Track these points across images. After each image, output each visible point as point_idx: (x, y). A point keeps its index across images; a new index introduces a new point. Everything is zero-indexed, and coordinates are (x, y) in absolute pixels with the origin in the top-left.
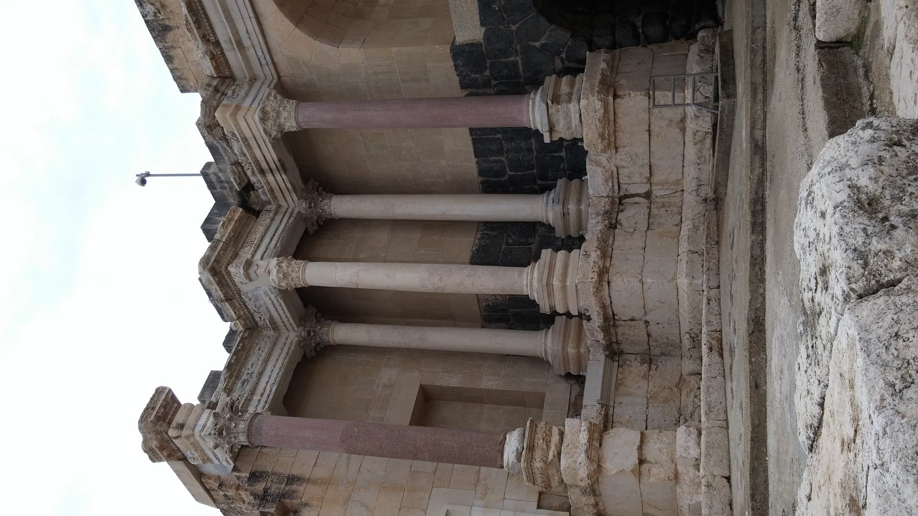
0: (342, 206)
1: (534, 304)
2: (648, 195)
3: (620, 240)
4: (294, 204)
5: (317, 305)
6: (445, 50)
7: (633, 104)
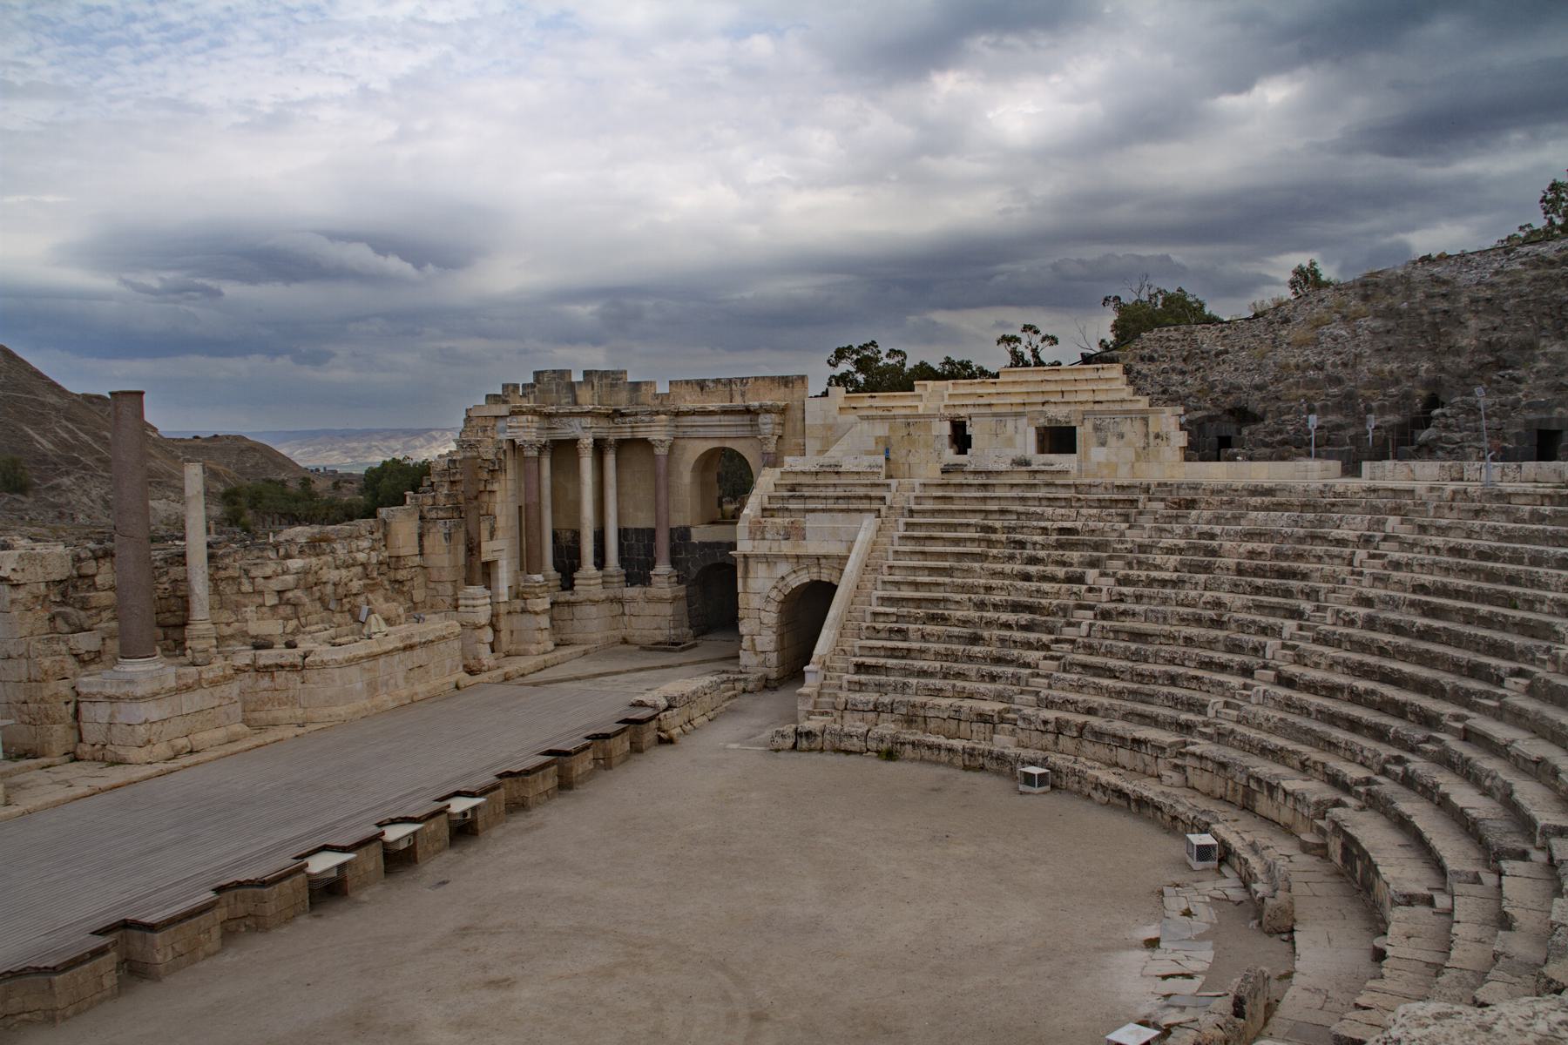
0: (610, 460)
2: (623, 614)
3: (606, 606)
4: (612, 438)
5: (563, 450)
7: (667, 609)
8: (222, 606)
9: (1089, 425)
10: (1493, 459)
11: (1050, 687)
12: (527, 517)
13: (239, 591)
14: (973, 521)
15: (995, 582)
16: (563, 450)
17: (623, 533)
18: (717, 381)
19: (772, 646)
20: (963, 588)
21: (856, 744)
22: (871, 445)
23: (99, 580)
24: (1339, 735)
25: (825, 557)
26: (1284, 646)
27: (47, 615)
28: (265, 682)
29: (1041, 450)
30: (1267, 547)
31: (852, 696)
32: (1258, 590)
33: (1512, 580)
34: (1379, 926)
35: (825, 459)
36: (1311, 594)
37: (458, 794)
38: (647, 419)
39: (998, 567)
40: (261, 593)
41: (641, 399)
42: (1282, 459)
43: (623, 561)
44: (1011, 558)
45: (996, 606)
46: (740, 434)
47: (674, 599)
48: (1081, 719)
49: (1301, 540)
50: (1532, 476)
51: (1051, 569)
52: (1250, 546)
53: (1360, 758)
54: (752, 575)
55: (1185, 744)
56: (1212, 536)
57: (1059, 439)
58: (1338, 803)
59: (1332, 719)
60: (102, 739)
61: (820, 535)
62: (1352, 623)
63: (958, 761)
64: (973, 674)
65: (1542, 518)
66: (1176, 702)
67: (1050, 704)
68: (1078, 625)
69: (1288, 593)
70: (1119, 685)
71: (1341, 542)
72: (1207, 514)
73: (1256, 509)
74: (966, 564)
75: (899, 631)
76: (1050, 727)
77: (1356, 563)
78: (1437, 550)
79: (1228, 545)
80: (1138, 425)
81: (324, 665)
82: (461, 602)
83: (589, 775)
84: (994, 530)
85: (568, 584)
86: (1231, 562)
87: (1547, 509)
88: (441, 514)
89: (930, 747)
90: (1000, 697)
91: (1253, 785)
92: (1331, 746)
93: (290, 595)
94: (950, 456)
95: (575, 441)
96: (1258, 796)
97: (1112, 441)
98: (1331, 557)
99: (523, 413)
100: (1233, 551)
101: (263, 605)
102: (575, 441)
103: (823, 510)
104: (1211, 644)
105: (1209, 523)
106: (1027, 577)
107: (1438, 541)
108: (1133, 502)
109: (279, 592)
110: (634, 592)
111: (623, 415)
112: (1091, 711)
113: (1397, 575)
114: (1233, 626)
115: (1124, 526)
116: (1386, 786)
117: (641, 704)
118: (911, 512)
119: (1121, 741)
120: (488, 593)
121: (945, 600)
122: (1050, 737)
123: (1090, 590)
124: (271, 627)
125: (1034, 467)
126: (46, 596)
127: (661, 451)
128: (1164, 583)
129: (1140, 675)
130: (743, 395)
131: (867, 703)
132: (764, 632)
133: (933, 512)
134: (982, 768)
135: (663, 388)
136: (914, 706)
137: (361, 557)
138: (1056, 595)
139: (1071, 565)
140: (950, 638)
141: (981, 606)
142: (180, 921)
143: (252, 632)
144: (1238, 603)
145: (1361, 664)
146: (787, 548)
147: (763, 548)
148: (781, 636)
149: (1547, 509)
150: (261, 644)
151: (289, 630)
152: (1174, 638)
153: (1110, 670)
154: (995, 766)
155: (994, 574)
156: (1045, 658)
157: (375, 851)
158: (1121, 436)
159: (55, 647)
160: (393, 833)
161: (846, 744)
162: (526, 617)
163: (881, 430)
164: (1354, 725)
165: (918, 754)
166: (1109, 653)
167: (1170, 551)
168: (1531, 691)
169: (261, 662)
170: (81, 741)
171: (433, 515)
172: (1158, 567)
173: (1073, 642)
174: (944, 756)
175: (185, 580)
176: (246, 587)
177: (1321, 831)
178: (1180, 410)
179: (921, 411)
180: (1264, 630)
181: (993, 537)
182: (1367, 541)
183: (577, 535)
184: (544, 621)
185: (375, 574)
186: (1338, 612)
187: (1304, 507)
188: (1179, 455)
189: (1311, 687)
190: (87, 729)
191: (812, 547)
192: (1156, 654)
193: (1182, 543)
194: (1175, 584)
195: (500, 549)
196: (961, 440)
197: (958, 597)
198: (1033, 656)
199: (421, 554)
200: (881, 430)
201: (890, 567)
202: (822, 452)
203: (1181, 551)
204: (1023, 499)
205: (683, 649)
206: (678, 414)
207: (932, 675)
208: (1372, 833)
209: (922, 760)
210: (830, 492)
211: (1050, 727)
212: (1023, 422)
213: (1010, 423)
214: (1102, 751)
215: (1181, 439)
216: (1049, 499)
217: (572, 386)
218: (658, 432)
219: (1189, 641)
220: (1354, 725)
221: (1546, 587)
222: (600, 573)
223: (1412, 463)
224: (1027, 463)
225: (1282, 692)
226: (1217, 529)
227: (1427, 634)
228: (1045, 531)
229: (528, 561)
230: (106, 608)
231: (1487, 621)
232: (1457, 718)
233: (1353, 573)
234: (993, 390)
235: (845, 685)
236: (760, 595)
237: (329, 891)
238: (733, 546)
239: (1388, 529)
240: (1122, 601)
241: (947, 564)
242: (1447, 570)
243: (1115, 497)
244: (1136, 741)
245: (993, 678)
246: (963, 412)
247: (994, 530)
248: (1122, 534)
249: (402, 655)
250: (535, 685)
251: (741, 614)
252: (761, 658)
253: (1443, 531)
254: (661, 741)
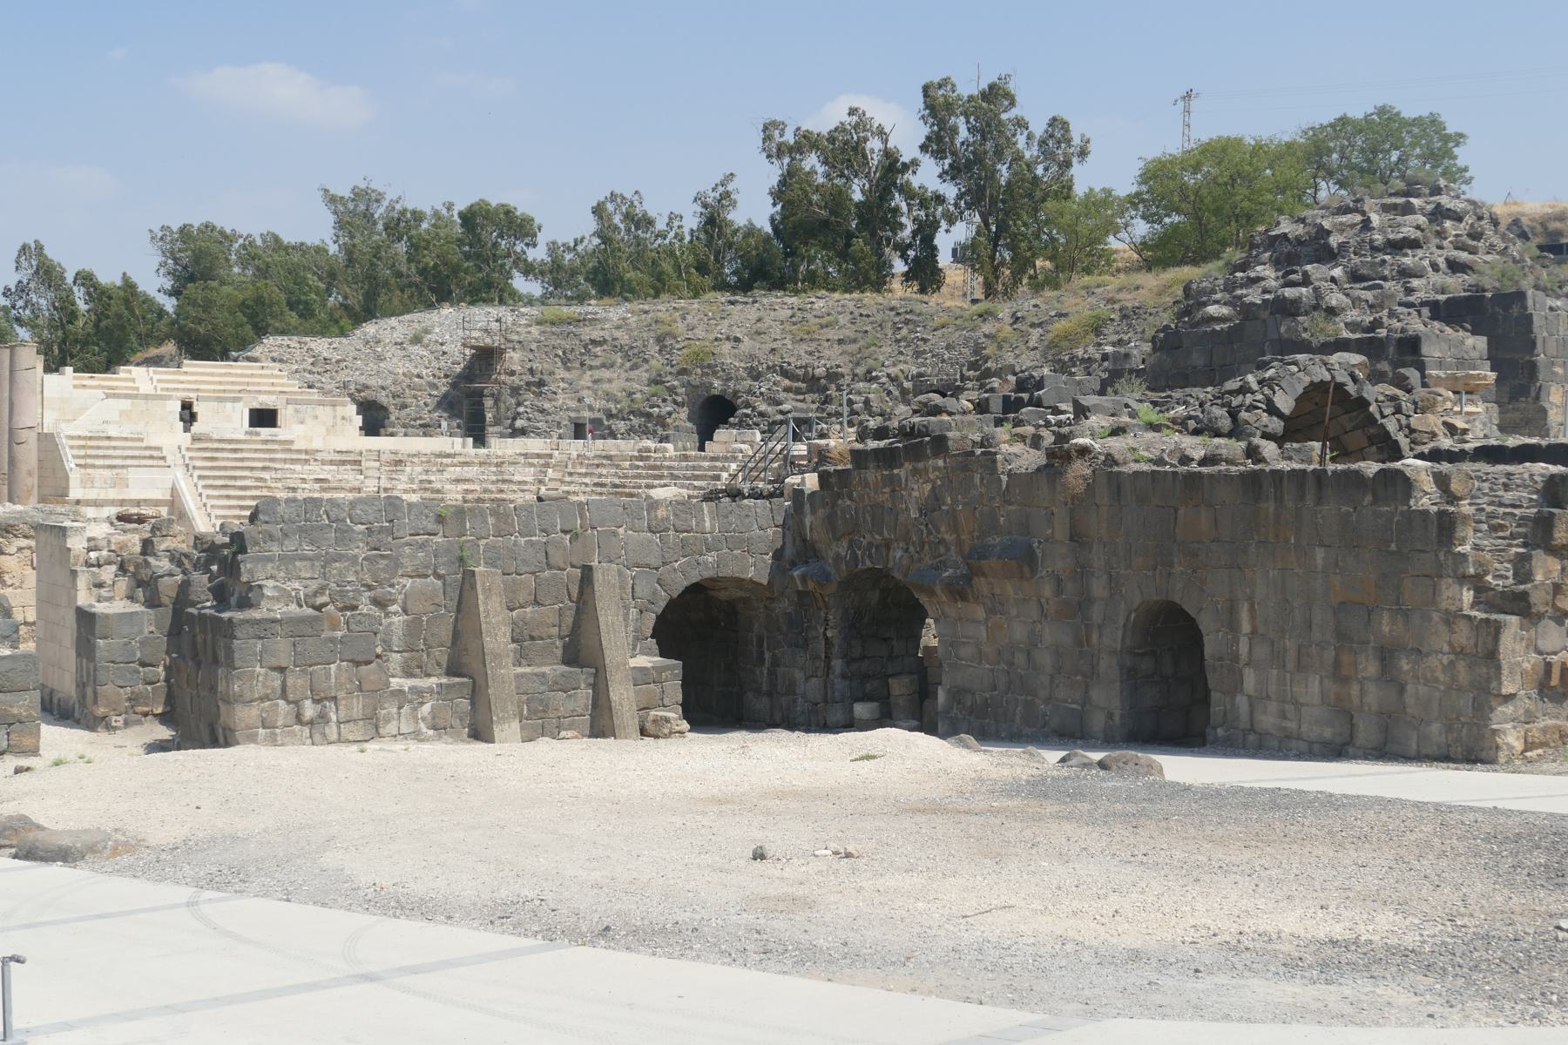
42: (425, 435)
57: (263, 418)
65: (638, 467)
71: (525, 483)
97: (309, 421)
107: (587, 480)
108: (358, 463)
125: (263, 437)
147: (92, 494)
167: (405, 491)
182: (541, 482)
187: (481, 464)
191: (134, 493)
196: (188, 414)
200: (125, 404)
212: (239, 405)
213: (229, 405)
215: (359, 420)
226: (433, 478)
246: (193, 395)
253: (586, 475)
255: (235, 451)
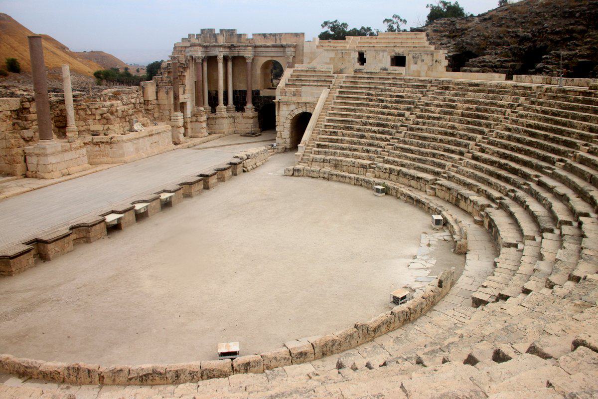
0: (230, 64)
1: (217, 106)
2: (234, 122)
4: (230, 56)
6: (259, 89)
7: (251, 121)
8: (80, 120)
9: (411, 56)
10: (563, 76)
11: (388, 155)
12: (198, 86)
13: (86, 114)
14: (364, 91)
15: (371, 115)
16: (211, 61)
17: (233, 91)
18: (271, 34)
19: (288, 136)
20: (359, 117)
21: (315, 175)
22: (328, 61)
23: (31, 110)
24: (493, 180)
25: (308, 103)
26: (476, 145)
27: (12, 123)
28: (97, 148)
29: (392, 65)
30: (473, 106)
31: (315, 156)
32: (469, 123)
33: (564, 124)
34: (497, 253)
35: (310, 66)
36: (488, 126)
37: (165, 191)
38: (243, 48)
39: (372, 109)
40: (94, 115)
41: (242, 41)
42: (483, 72)
43: (235, 102)
44: (378, 106)
45: (371, 124)
46: (279, 55)
47: (253, 117)
48: (398, 168)
49: (487, 104)
50: (577, 84)
51: (392, 111)
52: (467, 105)
53: (499, 189)
54: (281, 109)
55: (436, 180)
56: (454, 101)
57: (399, 61)
58: (489, 206)
59: (491, 174)
60: (34, 169)
61: (307, 94)
62: (502, 138)
63: (353, 182)
64: (360, 149)
66: (434, 164)
67: (388, 162)
68: (401, 132)
69: (480, 125)
70: (414, 156)
72: (453, 92)
73: (471, 91)
74: (360, 108)
75: (334, 132)
76: (387, 171)
77: (506, 114)
78: (537, 111)
79: (459, 105)
80: (430, 57)
81: (118, 142)
82: (172, 118)
83: (215, 185)
84: (372, 95)
85: (214, 111)
86: (459, 111)
87: (580, 97)
88: (164, 84)
89: (342, 177)
90: (369, 158)
91: (459, 197)
92: (489, 184)
93: (105, 115)
94: (357, 66)
95: (216, 57)
96: (461, 201)
98: (498, 111)
99: (195, 46)
100: (461, 107)
101: (95, 119)
102: (216, 57)
103: (309, 85)
104: (449, 143)
105: (453, 96)
106: (383, 114)
107: (538, 107)
108: (425, 87)
109: (101, 115)
110: (239, 114)
111: (235, 47)
112: (403, 165)
113: (521, 120)
114: (458, 136)
115: (421, 95)
116: (507, 201)
117: (237, 157)
118: (342, 87)
119: (413, 177)
120: (182, 114)
121: (352, 121)
122: (387, 175)
123: (406, 119)
124: (98, 127)
125: (389, 71)
126: (11, 116)
127: (249, 61)
128: (434, 118)
129: (422, 153)
130: (280, 40)
131: (321, 159)
132: (285, 131)
133: (349, 87)
134: (361, 185)
135: (250, 37)
136: (338, 161)
137: (133, 101)
138: (394, 121)
139: (400, 110)
140: (353, 136)
141: (365, 124)
142: (61, 238)
143: (91, 129)
144: (461, 127)
145: (504, 153)
146: (294, 99)
147: (284, 99)
148: (292, 132)
149: (580, 97)
150: (95, 133)
151: (105, 128)
152: (436, 140)
153: (411, 150)
154: (365, 185)
155: (371, 112)
156: (388, 145)
157: (132, 213)
158: (423, 61)
159: (15, 135)
160: (138, 207)
161: (312, 174)
162: (197, 123)
163: (332, 55)
164: (499, 177)
165: (337, 179)
166: (412, 144)
167: (437, 106)
168: (565, 168)
169: (95, 141)
170: (28, 170)
171: (161, 84)
172: (432, 112)
173: (398, 139)
174: (347, 180)
175: (65, 110)
176: (89, 112)
177: (482, 216)
178: (446, 51)
179: (348, 48)
180: (469, 139)
181: (371, 97)
182: (511, 106)
183: (217, 93)
184: (204, 125)
185: (139, 108)
186: (498, 133)
187: (490, 92)
188: (445, 69)
189: (485, 161)
190: (29, 165)
191: (304, 99)
192: (429, 145)
193: (442, 103)
194: (439, 119)
195: (187, 97)
196: (362, 59)
197: (357, 120)
198: (383, 143)
199: (157, 99)
200: (332, 55)
201: (332, 108)
202: (309, 63)
203: (441, 106)
204: (384, 84)
205: (256, 136)
206: (256, 47)
207: (345, 149)
208: (499, 218)
209: (339, 181)
210: (312, 79)
211: (387, 171)
212: (386, 54)
214: (406, 181)
215: (446, 63)
216: (394, 84)
217: (215, 35)
218: (248, 54)
219: (441, 141)
220: (499, 177)
221: (576, 128)
222: (226, 107)
223: (533, 76)
224: (386, 69)
225: (474, 162)
226: (456, 98)
227: (530, 143)
228: (391, 96)
229: (198, 102)
230: (34, 120)
231: (553, 140)
232: (536, 176)
233: (505, 118)
234: (375, 41)
235: (313, 152)
236: (284, 117)
237: (114, 228)
238: (274, 98)
239: (520, 102)
240: (418, 124)
241: (353, 107)
242: (540, 119)
243: (418, 84)
244: (418, 178)
245: (368, 151)
246: (363, 49)
247: (372, 95)
248: (420, 99)
249: (148, 138)
250: (199, 149)
251: (277, 124)
252: (284, 140)
253: (540, 104)
254: (244, 171)
255: (370, 78)
